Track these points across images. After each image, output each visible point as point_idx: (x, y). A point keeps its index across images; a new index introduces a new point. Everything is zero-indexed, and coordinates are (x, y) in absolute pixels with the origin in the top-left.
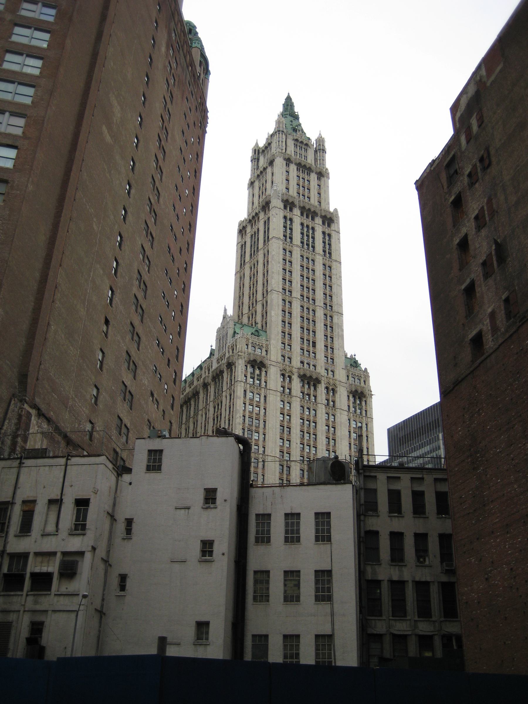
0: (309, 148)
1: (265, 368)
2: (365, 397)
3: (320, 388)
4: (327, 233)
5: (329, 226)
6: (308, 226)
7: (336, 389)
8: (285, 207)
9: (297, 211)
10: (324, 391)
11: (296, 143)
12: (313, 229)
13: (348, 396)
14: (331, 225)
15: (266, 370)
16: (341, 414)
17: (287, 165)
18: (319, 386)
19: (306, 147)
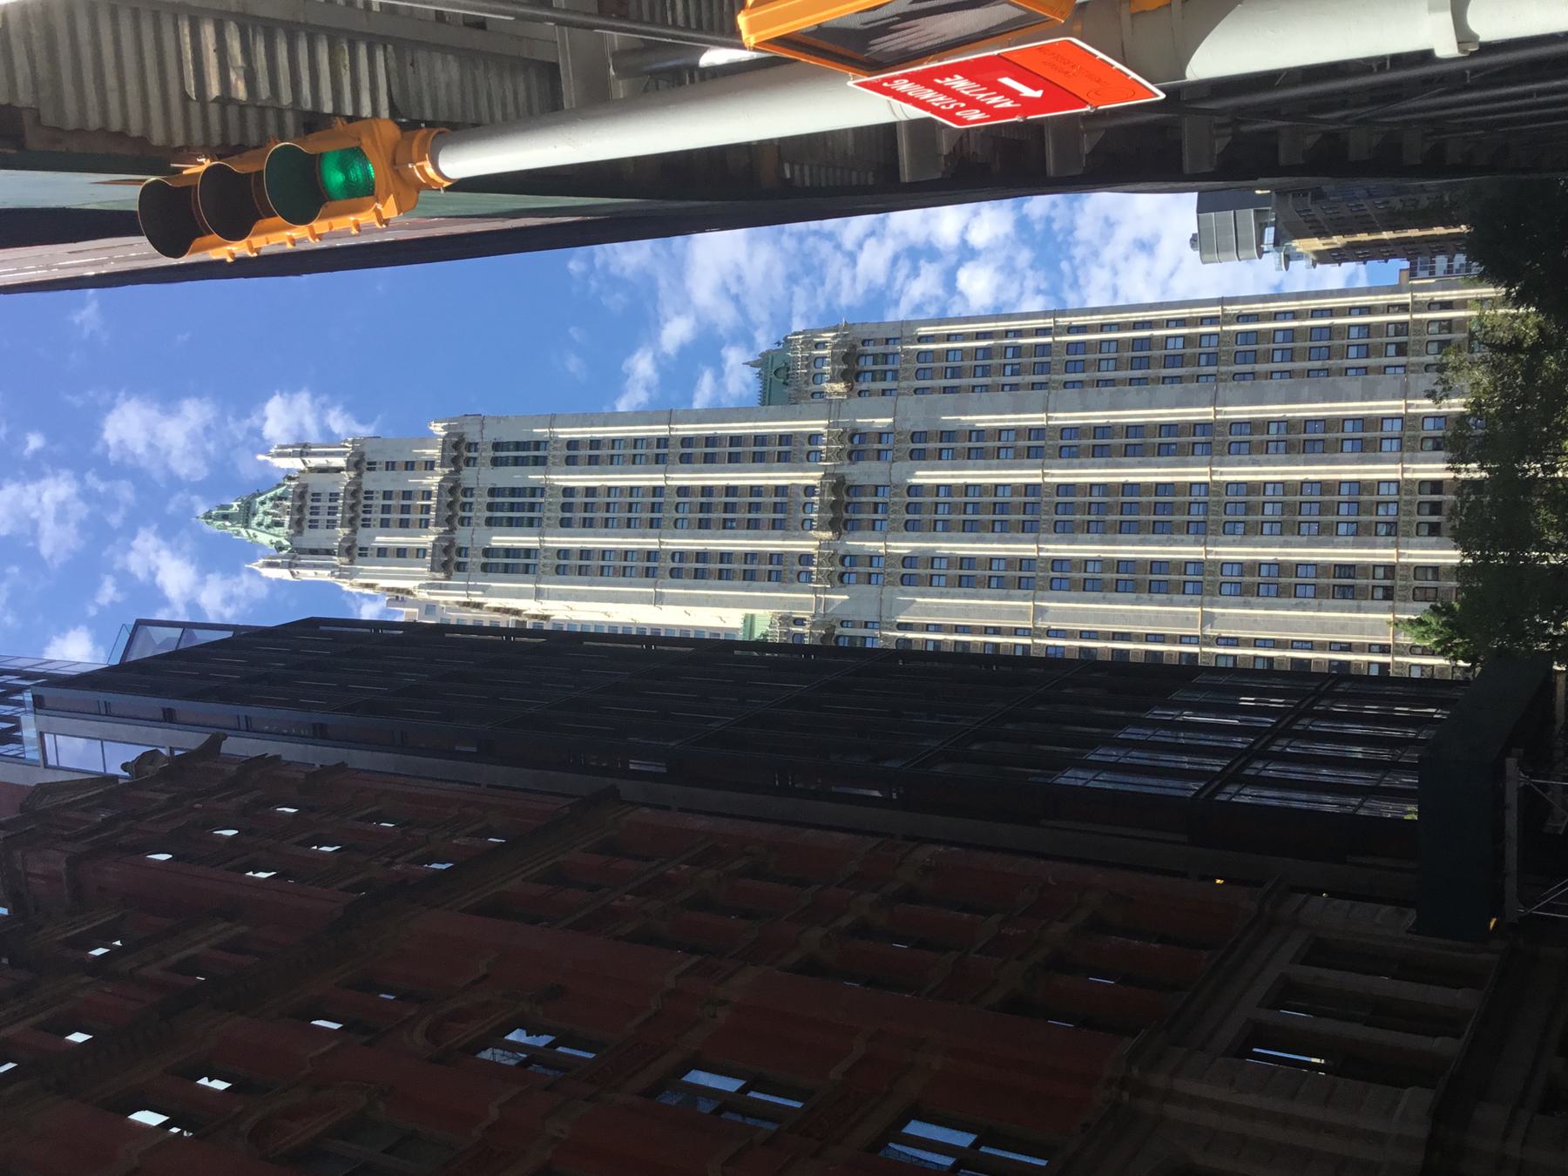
0: (310, 490)
1: (835, 627)
2: (854, 347)
3: (855, 478)
4: (492, 454)
5: (472, 446)
6: (490, 507)
7: (848, 430)
8: (461, 567)
9: (463, 536)
10: (863, 466)
11: (306, 524)
12: (493, 492)
13: (860, 393)
14: (470, 441)
15: (838, 625)
16: (906, 420)
17: (363, 552)
18: (849, 480)
19: (308, 498)
